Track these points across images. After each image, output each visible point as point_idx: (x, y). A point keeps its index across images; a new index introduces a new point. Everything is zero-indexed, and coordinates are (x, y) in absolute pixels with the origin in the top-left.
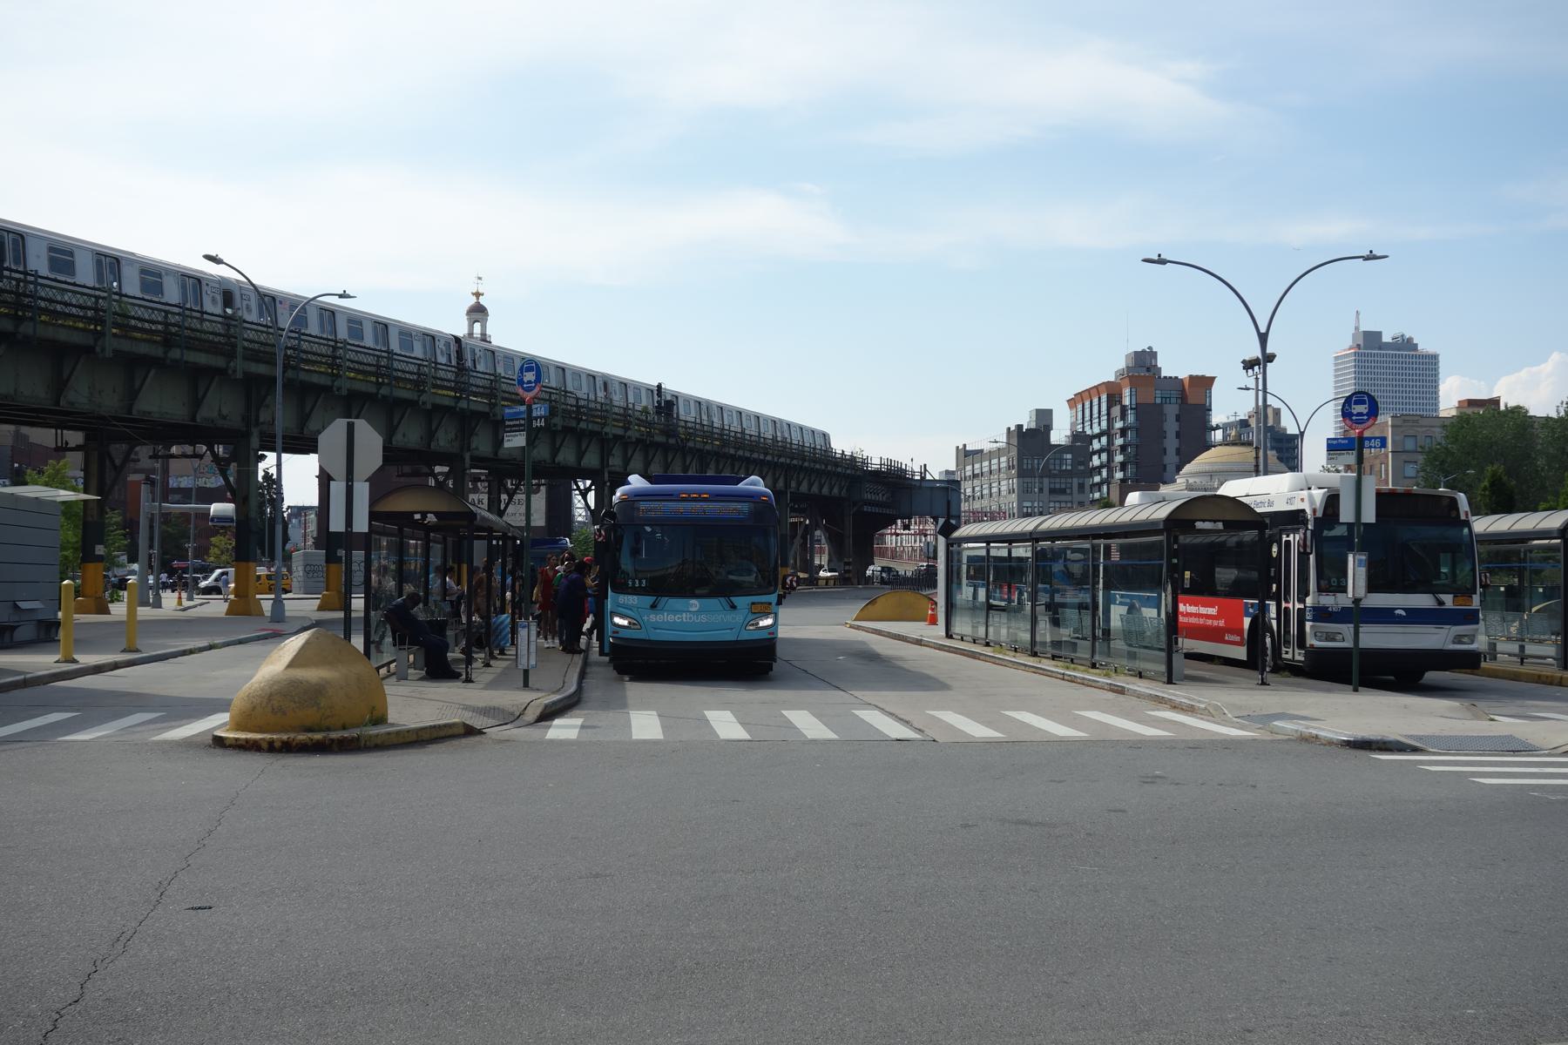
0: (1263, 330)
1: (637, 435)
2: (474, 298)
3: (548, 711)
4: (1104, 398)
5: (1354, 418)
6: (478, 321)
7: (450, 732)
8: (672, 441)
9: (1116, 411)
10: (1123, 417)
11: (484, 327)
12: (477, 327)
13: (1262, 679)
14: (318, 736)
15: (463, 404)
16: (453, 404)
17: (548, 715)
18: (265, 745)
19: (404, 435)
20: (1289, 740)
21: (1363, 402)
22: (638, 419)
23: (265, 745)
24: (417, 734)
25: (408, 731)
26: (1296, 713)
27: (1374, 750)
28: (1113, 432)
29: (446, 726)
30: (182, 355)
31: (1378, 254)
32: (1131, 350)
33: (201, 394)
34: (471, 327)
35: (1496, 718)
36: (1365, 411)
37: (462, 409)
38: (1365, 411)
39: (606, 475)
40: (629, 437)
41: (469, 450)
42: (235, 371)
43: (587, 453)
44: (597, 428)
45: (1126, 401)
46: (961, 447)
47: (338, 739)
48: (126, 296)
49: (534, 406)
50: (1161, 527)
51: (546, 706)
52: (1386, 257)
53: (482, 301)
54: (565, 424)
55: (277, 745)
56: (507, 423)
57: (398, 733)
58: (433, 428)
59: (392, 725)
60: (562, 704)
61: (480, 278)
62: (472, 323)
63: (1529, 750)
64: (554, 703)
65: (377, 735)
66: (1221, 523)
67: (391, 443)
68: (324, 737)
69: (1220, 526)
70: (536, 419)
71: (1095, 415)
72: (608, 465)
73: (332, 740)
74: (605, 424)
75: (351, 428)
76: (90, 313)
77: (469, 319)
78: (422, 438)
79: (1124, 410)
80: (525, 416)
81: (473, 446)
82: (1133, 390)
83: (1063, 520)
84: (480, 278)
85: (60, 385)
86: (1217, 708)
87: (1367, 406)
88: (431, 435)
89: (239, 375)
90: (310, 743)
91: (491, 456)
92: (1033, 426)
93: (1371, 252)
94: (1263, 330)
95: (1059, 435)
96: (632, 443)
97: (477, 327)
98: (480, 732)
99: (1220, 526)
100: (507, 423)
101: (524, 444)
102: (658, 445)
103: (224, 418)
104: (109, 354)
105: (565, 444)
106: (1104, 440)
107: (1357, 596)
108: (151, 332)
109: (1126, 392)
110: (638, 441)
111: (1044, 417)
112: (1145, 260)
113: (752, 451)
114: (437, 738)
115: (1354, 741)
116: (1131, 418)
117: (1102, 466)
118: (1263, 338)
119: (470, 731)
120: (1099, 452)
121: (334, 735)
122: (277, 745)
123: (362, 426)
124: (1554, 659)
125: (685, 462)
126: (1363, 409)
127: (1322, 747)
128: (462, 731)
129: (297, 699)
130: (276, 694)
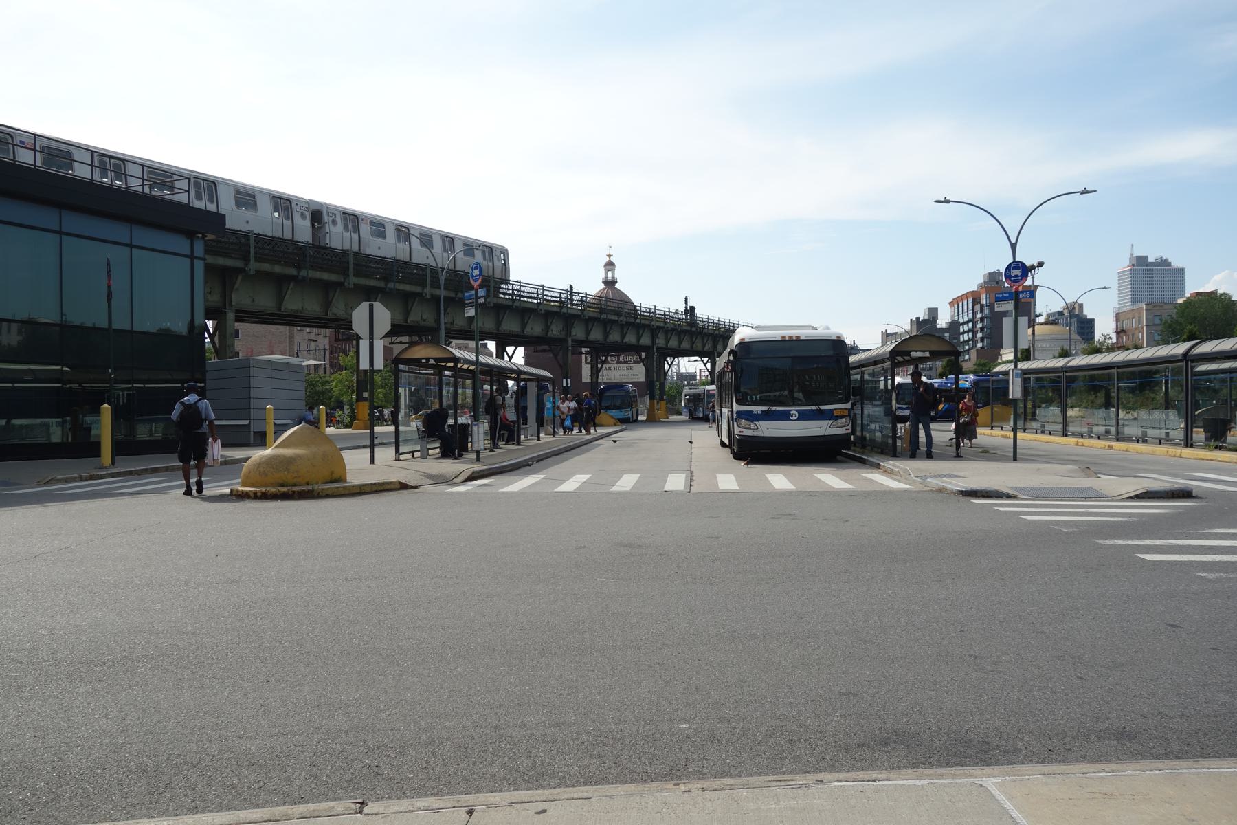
0: (1013, 241)
1: (672, 326)
2: (608, 259)
3: (474, 475)
4: (970, 300)
5: (1013, 279)
6: (609, 270)
7: (388, 487)
8: (694, 329)
9: (978, 307)
10: (982, 311)
11: (613, 274)
12: (610, 274)
13: (957, 454)
15: (564, 310)
16: (558, 310)
17: (471, 478)
18: (252, 495)
19: (532, 329)
20: (931, 490)
21: (1018, 268)
22: (673, 317)
23: (252, 495)
24: (360, 488)
25: (353, 487)
26: (959, 474)
27: (979, 497)
28: (976, 320)
29: (384, 483)
30: (394, 286)
31: (1090, 190)
32: (987, 272)
33: (409, 308)
34: (606, 273)
35: (1102, 476)
36: (1020, 274)
37: (564, 313)
38: (1020, 274)
39: (655, 349)
40: (667, 327)
42: (426, 294)
43: (627, 335)
44: (647, 322)
45: (984, 302)
46: (884, 331)
47: (298, 492)
48: (297, 242)
49: (479, 290)
50: (888, 356)
51: (474, 473)
52: (1095, 191)
53: (612, 259)
54: (627, 320)
55: (259, 494)
56: (466, 302)
57: (345, 488)
58: (549, 324)
59: (350, 483)
60: (491, 471)
61: (610, 247)
63: (1098, 496)
64: (483, 470)
65: (323, 490)
66: (928, 353)
67: (523, 332)
68: (289, 490)
69: (927, 354)
70: (480, 298)
71: (965, 310)
73: (294, 492)
74: (652, 320)
75: (371, 307)
77: (605, 270)
78: (542, 330)
79: (982, 307)
80: (474, 297)
81: (573, 333)
82: (988, 295)
83: (863, 357)
84: (610, 247)
85: (327, 304)
86: (906, 471)
87: (1020, 270)
88: (547, 328)
89: (429, 296)
90: (279, 494)
91: (584, 339)
92: (926, 318)
93: (1085, 189)
94: (1013, 241)
95: (943, 321)
96: (668, 330)
97: (610, 274)
98: (415, 488)
99: (927, 354)
100: (466, 302)
101: (474, 314)
102: (686, 332)
103: (424, 320)
104: (351, 286)
105: (629, 331)
106: (971, 324)
107: (1015, 397)
109: (984, 296)
110: (673, 330)
111: (933, 313)
112: (936, 201)
113: (386, 279)
114: (376, 491)
115: (965, 491)
116: (986, 311)
117: (969, 340)
118: (1014, 247)
119: (404, 486)
120: (968, 332)
121: (295, 489)
122: (259, 494)
123: (379, 307)
124: (1181, 440)
125: (639, 333)
126: (1018, 272)
127: (948, 495)
128: (399, 487)
129: (274, 467)
130: (263, 463)
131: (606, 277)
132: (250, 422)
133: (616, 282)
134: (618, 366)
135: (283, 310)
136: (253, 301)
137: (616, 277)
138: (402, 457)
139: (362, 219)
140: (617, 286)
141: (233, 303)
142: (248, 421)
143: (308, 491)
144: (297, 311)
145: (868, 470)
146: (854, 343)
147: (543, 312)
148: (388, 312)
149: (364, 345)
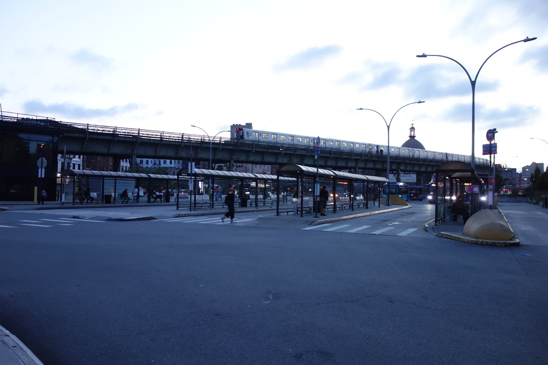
0: (388, 125)
8: (380, 159)
19: (282, 160)
37: (296, 154)
41: (303, 163)
53: (414, 126)
61: (413, 120)
62: (411, 132)
72: (357, 166)
75: (42, 159)
76: (180, 138)
78: (288, 161)
81: (304, 162)
84: (413, 120)
97: (412, 132)
103: (224, 158)
108: (198, 141)
118: (388, 127)
123: (44, 159)
131: (411, 134)
133: (415, 137)
134: (404, 175)
137: (415, 133)
140: (415, 138)
141: (135, 153)
144: (164, 155)
146: (506, 166)
147: (283, 154)
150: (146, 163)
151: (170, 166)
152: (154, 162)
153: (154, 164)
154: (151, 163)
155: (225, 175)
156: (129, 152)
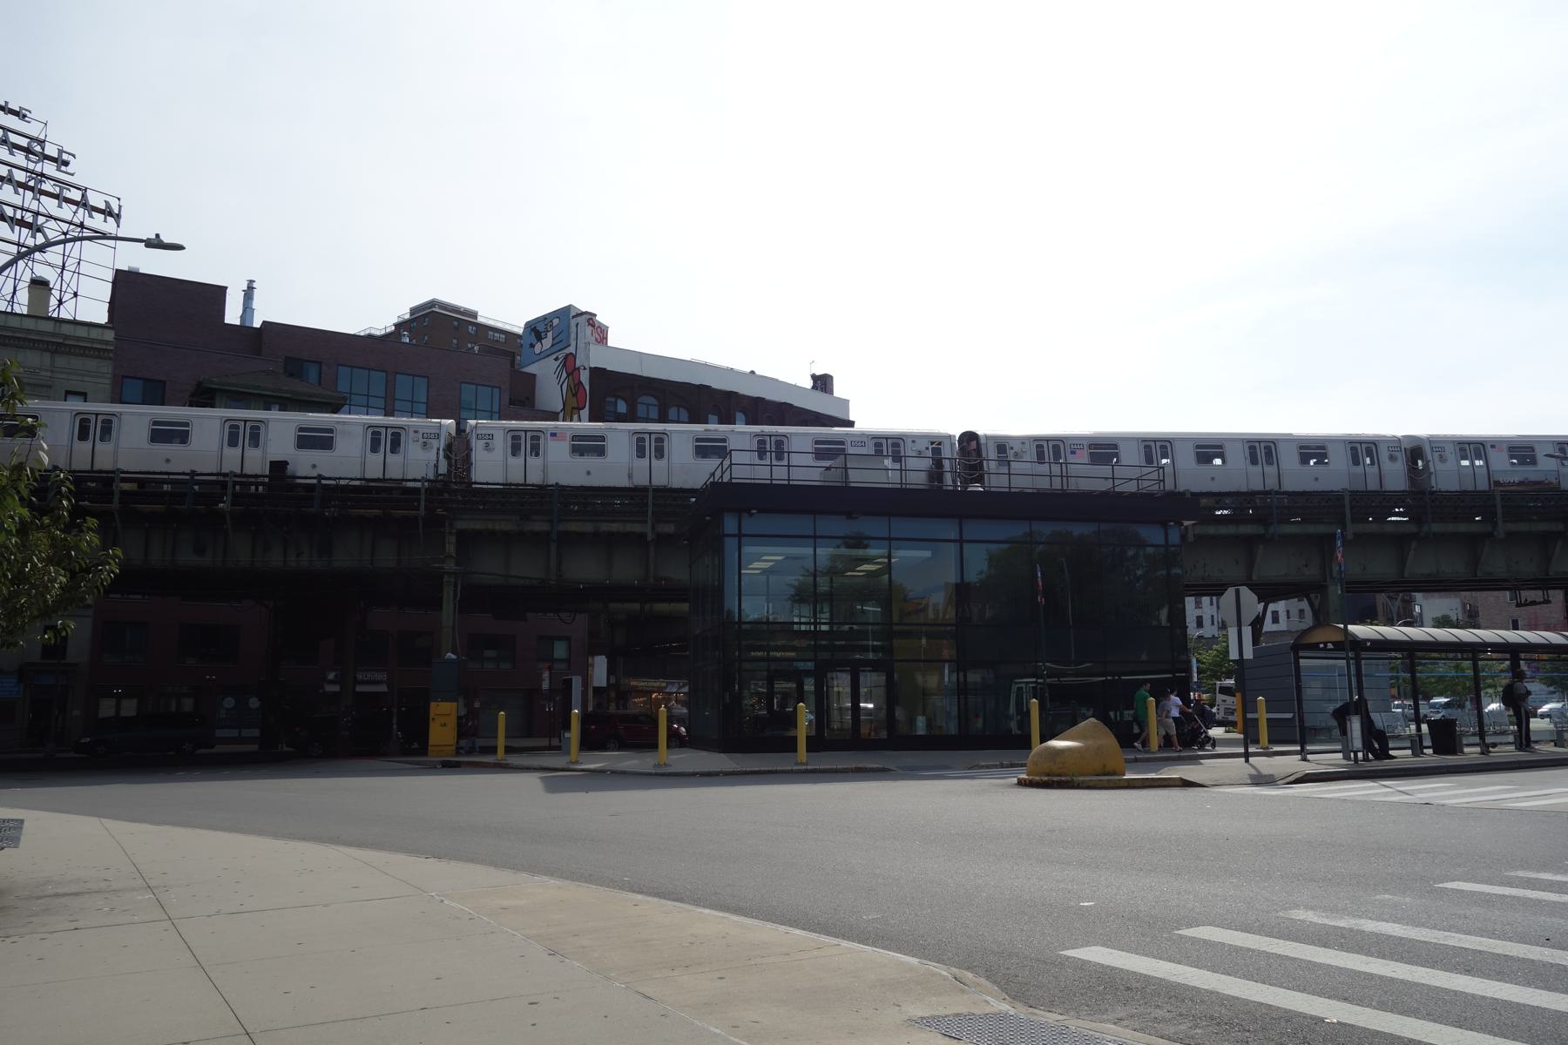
7: (1166, 783)
14: (1045, 778)
47: (1057, 781)
73: (1053, 781)
75: (1237, 592)
121: (1055, 779)
128: (1181, 784)
132: (1294, 717)
135: (1406, 575)
136: (1364, 569)
138: (1309, 757)
139: (1493, 446)
142: (1292, 715)
143: (1067, 782)
145: (1430, 780)
148: (1253, 595)
149: (1232, 632)
150: (1195, 625)
151: (1275, 628)
152: (1220, 620)
153: (1221, 625)
154: (1213, 624)
155: (1503, 641)
156: (1312, 573)
